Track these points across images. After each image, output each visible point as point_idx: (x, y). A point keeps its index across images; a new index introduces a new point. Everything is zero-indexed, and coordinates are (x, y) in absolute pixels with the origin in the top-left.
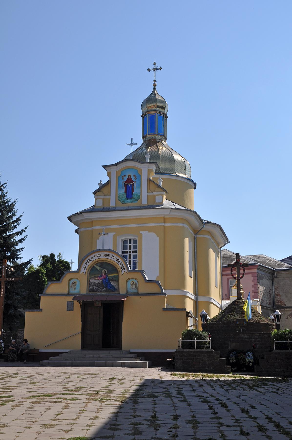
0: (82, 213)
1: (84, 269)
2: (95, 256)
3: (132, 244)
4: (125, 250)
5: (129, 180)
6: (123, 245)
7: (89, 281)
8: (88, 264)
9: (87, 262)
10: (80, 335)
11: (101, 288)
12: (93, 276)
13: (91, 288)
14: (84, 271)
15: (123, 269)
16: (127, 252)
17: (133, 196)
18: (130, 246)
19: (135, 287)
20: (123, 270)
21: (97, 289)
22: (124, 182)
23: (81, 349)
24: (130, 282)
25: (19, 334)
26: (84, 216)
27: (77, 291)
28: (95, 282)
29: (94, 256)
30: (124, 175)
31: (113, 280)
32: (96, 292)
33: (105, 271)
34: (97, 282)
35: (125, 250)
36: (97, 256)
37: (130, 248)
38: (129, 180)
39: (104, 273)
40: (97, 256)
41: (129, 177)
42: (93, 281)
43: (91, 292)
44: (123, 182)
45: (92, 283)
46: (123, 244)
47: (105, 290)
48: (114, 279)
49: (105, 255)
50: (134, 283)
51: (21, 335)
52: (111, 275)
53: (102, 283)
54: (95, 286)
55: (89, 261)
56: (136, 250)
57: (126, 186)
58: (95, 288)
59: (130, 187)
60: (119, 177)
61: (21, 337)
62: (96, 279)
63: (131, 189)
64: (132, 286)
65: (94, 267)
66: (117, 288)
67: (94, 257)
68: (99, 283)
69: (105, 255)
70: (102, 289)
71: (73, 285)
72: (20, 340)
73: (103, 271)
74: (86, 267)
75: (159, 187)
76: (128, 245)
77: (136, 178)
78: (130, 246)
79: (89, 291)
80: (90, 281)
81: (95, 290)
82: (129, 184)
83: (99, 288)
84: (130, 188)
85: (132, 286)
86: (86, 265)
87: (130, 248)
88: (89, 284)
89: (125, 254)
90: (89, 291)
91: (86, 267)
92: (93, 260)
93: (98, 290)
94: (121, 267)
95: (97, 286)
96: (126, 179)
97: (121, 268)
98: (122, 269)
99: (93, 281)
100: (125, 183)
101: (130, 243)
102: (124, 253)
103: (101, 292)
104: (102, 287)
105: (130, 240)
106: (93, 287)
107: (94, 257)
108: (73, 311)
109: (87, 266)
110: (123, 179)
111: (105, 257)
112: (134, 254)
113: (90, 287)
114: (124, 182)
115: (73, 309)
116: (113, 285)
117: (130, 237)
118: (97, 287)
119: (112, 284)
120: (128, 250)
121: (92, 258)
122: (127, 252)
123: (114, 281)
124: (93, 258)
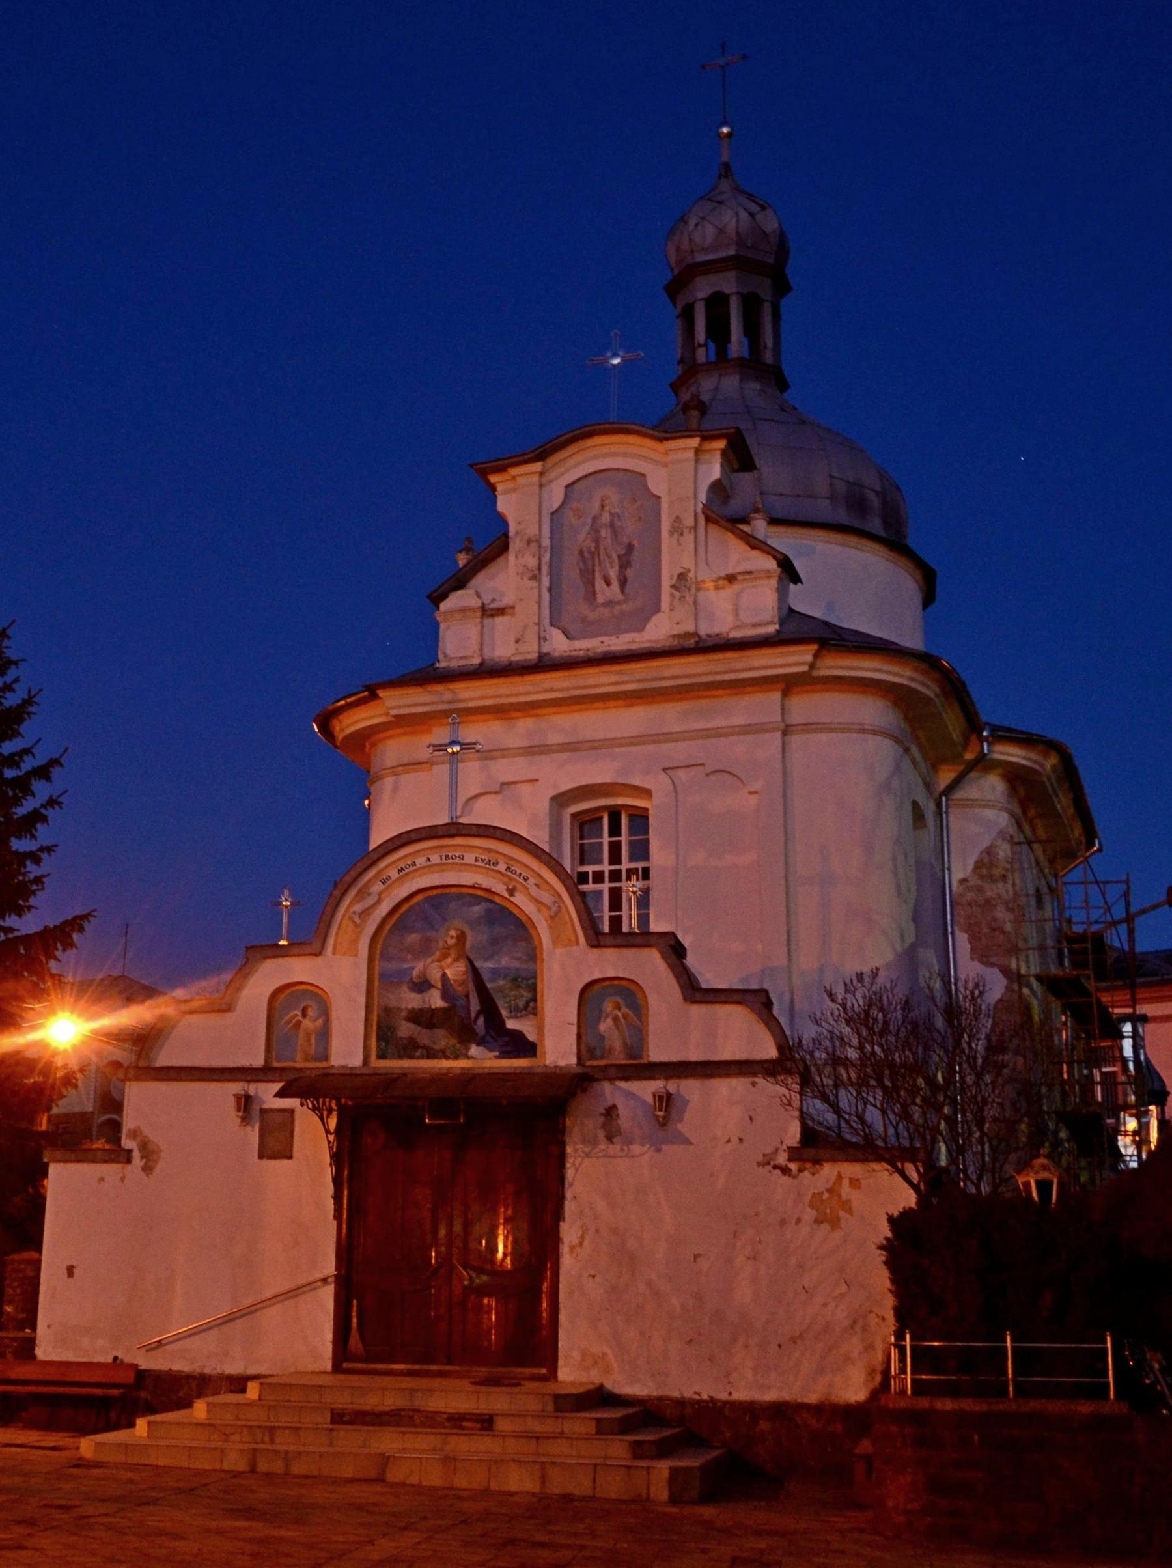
0: (381, 693)
3: (624, 839)
4: (590, 869)
6: (582, 845)
10: (328, 1294)
16: (599, 877)
18: (615, 849)
23: (337, 1368)
35: (590, 869)
37: (615, 858)
46: (582, 838)
60: (552, 514)
76: (606, 839)
78: (615, 849)
87: (615, 858)
101: (615, 830)
102: (587, 883)
105: (615, 814)
108: (290, 1157)
115: (291, 1150)
120: (606, 867)
122: (599, 877)
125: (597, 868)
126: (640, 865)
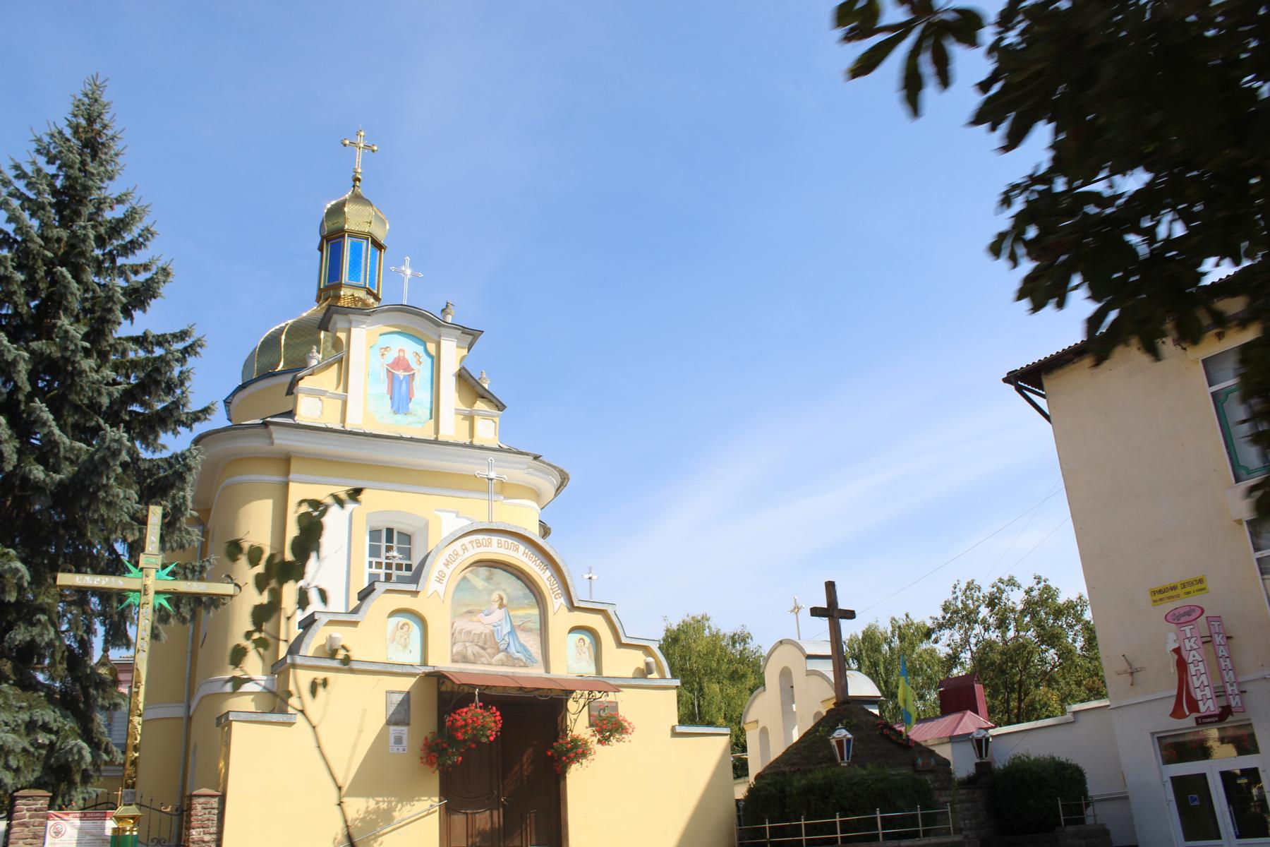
1: (439, 580)
2: (474, 544)
5: (400, 363)
7: (453, 624)
8: (452, 567)
9: (449, 559)
11: (490, 650)
12: (464, 610)
13: (457, 648)
14: (440, 588)
15: (557, 596)
17: (411, 405)
19: (587, 654)
20: (557, 599)
21: (478, 653)
22: (387, 365)
24: (576, 636)
25: (199, 807)
26: (274, 436)
27: (412, 656)
28: (470, 632)
29: (471, 542)
30: (387, 347)
31: (524, 630)
32: (474, 663)
33: (501, 599)
34: (478, 631)
36: (479, 544)
38: (400, 363)
39: (498, 603)
40: (479, 543)
41: (402, 354)
42: (465, 624)
43: (456, 662)
44: (382, 364)
45: (460, 632)
47: (501, 660)
48: (525, 624)
49: (503, 543)
50: (584, 644)
51: (210, 813)
52: (520, 613)
53: (493, 635)
54: (471, 642)
55: (455, 557)
56: (408, 562)
57: (392, 377)
58: (471, 650)
59: (401, 381)
61: (208, 820)
62: (474, 619)
63: (404, 386)
64: (580, 652)
65: (464, 578)
66: (536, 655)
67: (469, 546)
68: (482, 633)
69: (503, 543)
70: (494, 655)
71: (400, 633)
72: (205, 833)
73: (495, 596)
74: (447, 578)
75: (483, 397)
77: (420, 363)
79: (454, 661)
80: (455, 625)
81: (472, 658)
82: (401, 374)
83: (483, 651)
84: (401, 385)
85: (580, 652)
86: (445, 570)
88: (453, 635)
89: (374, 570)
90: (454, 661)
91: (447, 578)
92: (467, 554)
93: (481, 656)
94: (550, 587)
95: (476, 645)
96: (391, 357)
97: (551, 591)
98: (553, 595)
99: (465, 624)
100: (387, 369)
101: (390, 538)
103: (490, 664)
104: (493, 648)
105: (390, 531)
106: (466, 647)
107: (469, 546)
109: (448, 572)
110: (383, 355)
111: (502, 550)
112: (400, 573)
113: (454, 644)
114: (387, 365)
115: (409, 719)
116: (525, 644)
117: (390, 526)
118: (478, 646)
119: (522, 641)
121: (465, 549)
123: (528, 631)
124: (466, 549)
125: (378, 560)
126: (404, 562)
